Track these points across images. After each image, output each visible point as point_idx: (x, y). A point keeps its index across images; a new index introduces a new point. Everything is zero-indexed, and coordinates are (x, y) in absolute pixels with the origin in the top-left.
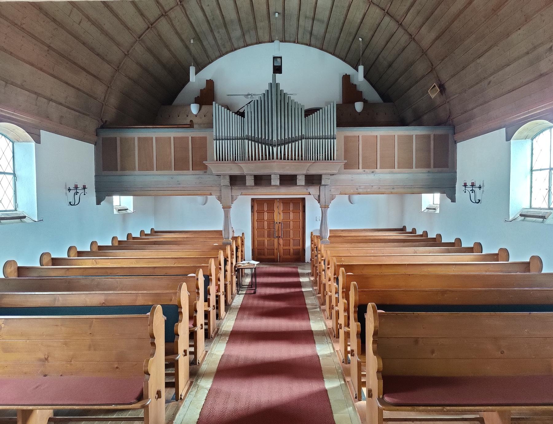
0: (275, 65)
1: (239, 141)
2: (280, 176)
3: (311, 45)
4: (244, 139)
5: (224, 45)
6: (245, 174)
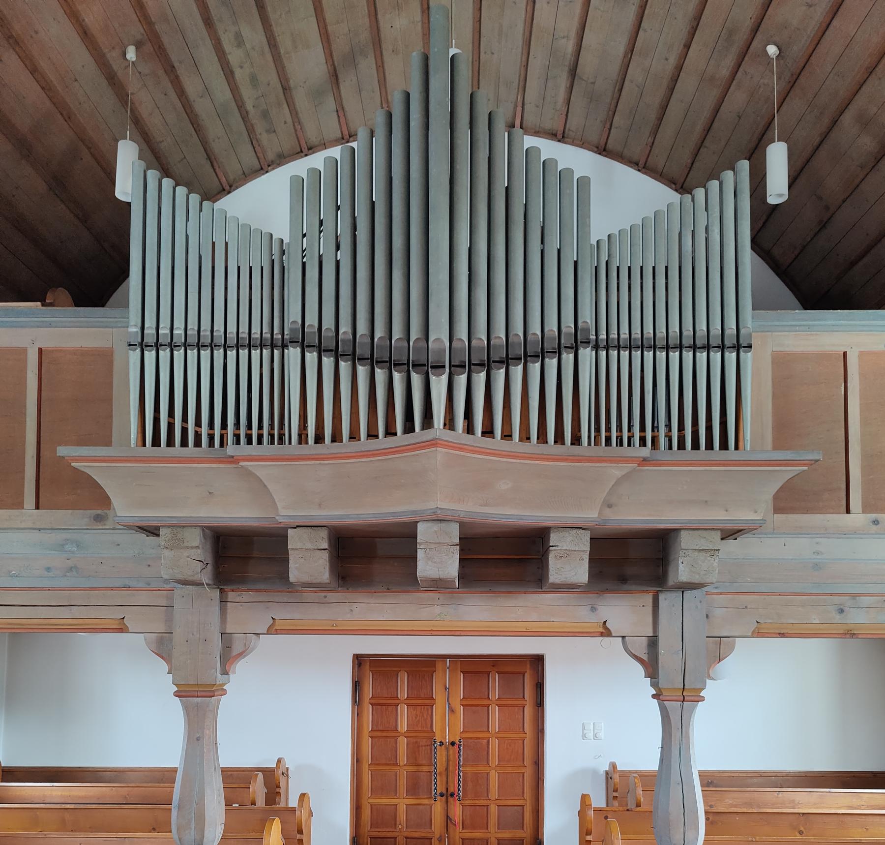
2: (463, 525)
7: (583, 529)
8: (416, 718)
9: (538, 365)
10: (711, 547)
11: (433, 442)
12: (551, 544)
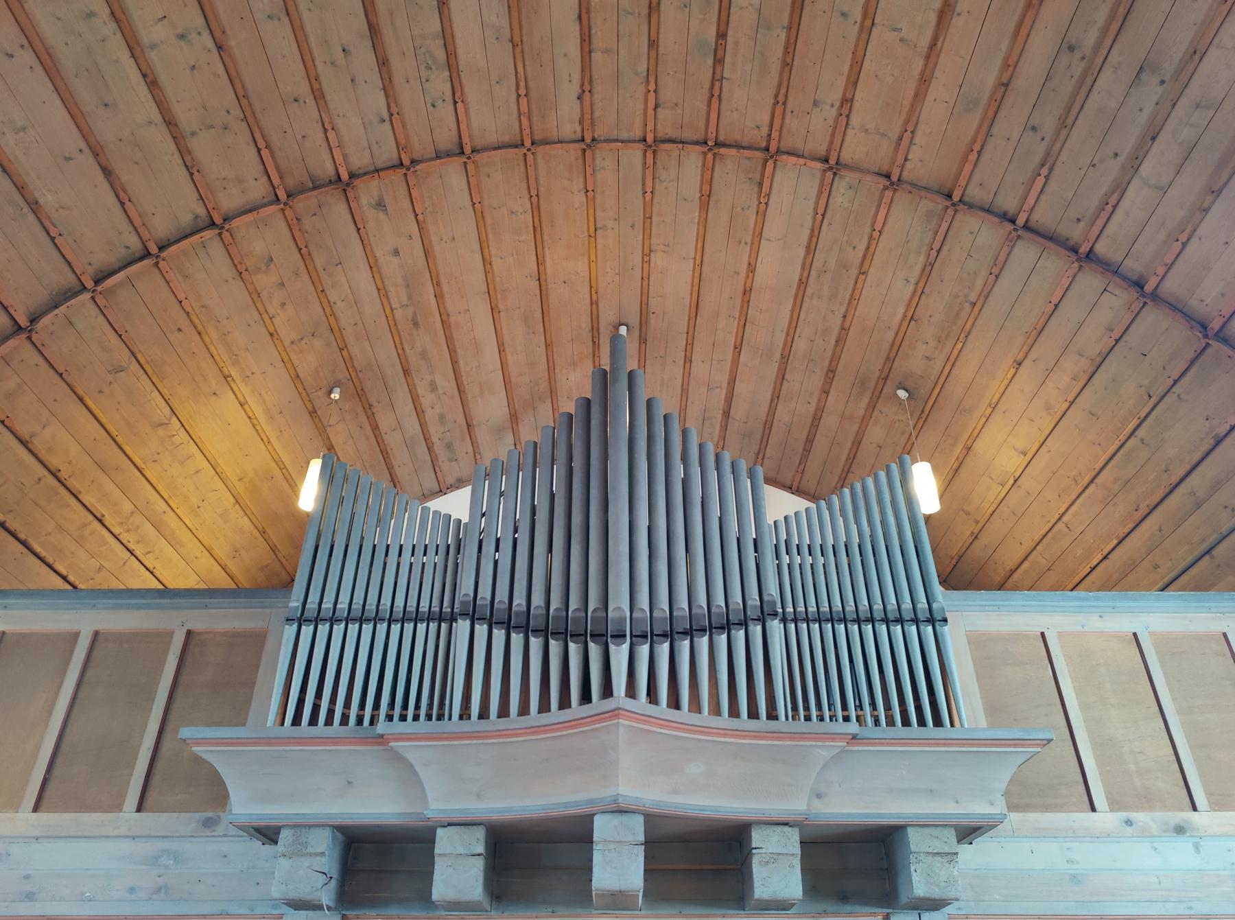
2: (651, 819)
5: (449, 446)
7: (790, 826)
9: (724, 637)
10: (947, 850)
11: (616, 712)
12: (754, 846)
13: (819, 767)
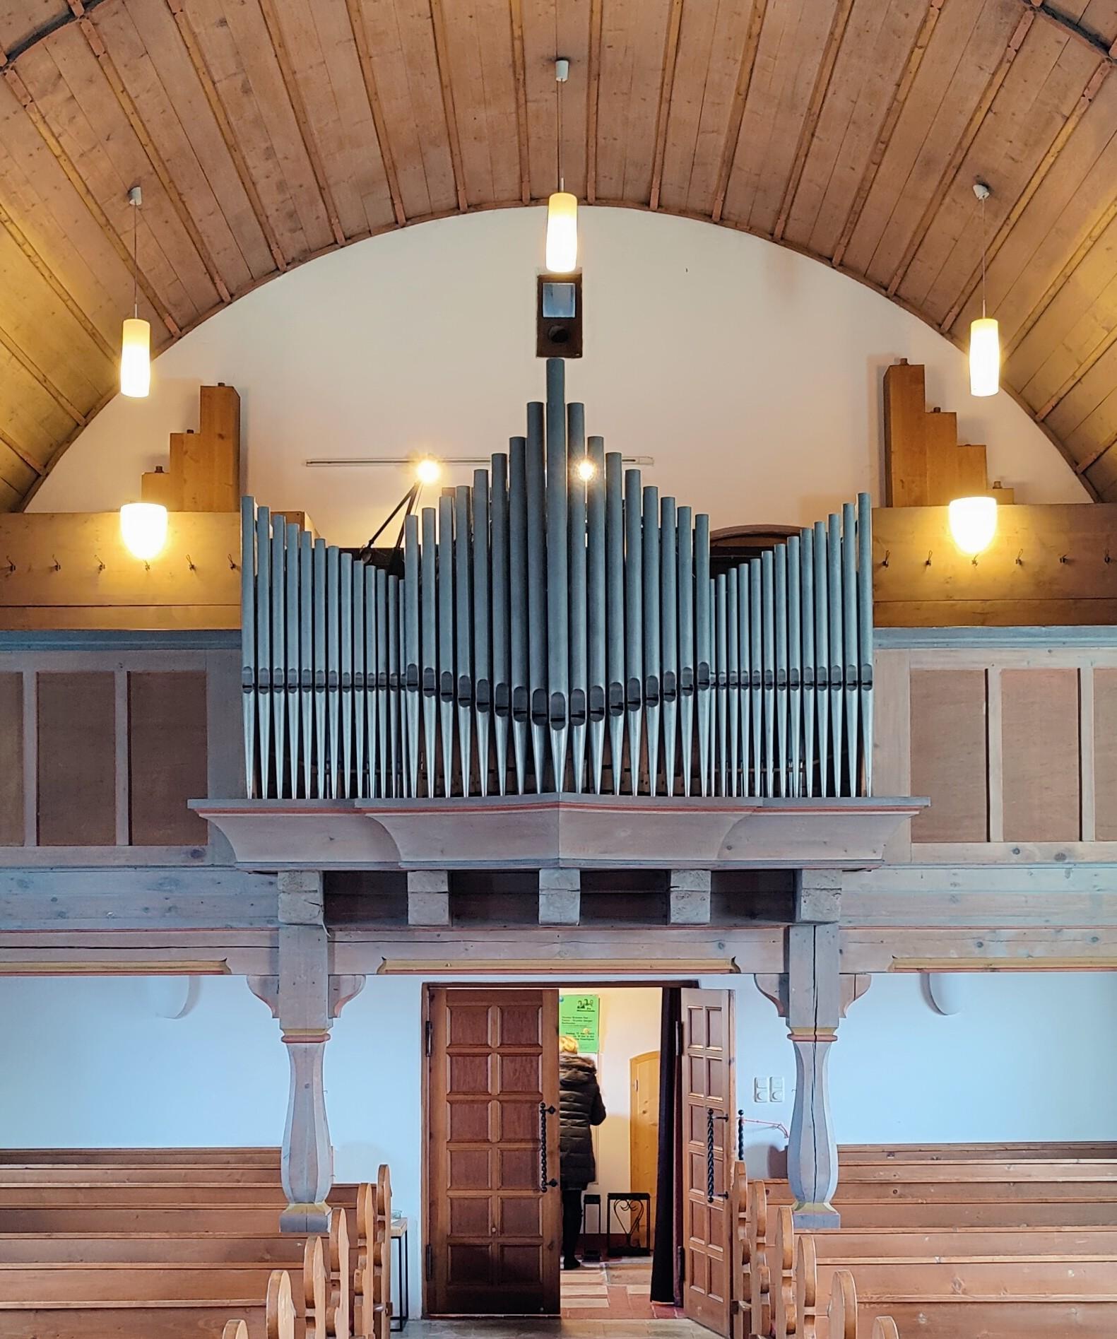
0: (545, 315)
1: (372, 695)
2: (586, 874)
3: (728, 220)
4: (400, 687)
6: (404, 867)
8: (515, 1074)
12: (672, 885)
13: (728, 829)
